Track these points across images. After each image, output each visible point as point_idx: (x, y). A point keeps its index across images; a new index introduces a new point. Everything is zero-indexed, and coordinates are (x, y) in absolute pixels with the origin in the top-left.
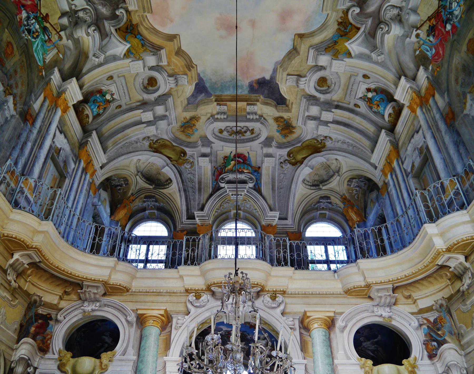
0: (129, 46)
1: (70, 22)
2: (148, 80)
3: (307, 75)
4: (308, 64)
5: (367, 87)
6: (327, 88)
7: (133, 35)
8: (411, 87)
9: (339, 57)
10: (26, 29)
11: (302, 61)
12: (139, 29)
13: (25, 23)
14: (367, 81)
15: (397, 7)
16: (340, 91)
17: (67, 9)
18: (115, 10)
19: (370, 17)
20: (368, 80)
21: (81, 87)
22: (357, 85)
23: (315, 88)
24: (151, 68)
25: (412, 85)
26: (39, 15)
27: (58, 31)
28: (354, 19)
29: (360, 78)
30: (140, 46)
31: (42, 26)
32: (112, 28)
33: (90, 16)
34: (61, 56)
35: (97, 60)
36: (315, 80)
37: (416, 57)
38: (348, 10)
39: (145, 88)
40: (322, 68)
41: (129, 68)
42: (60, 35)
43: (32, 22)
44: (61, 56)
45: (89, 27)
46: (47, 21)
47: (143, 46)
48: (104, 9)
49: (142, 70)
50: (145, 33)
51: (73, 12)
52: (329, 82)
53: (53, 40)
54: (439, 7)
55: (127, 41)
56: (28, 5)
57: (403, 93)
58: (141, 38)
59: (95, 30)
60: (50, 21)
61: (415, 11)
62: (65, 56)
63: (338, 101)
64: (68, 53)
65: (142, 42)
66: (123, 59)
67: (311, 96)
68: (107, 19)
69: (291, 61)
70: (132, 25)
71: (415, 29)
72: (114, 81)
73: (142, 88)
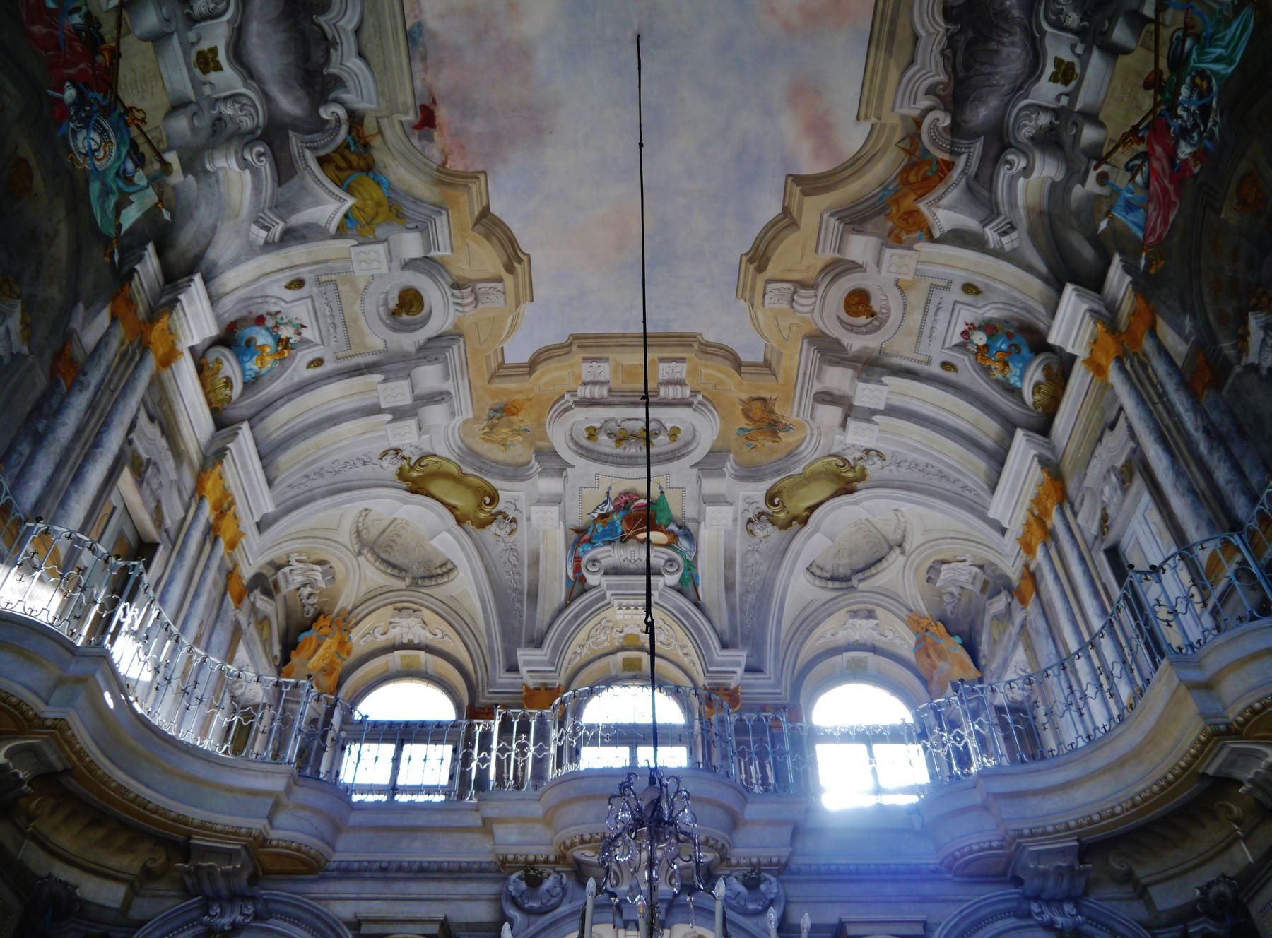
13: (1195, 135)
26: (1163, 107)
27: (1152, 27)
31: (1175, 78)
42: (1157, 11)
43: (1185, 114)
46: (1157, 71)
54: (118, 98)
60: (1152, 68)
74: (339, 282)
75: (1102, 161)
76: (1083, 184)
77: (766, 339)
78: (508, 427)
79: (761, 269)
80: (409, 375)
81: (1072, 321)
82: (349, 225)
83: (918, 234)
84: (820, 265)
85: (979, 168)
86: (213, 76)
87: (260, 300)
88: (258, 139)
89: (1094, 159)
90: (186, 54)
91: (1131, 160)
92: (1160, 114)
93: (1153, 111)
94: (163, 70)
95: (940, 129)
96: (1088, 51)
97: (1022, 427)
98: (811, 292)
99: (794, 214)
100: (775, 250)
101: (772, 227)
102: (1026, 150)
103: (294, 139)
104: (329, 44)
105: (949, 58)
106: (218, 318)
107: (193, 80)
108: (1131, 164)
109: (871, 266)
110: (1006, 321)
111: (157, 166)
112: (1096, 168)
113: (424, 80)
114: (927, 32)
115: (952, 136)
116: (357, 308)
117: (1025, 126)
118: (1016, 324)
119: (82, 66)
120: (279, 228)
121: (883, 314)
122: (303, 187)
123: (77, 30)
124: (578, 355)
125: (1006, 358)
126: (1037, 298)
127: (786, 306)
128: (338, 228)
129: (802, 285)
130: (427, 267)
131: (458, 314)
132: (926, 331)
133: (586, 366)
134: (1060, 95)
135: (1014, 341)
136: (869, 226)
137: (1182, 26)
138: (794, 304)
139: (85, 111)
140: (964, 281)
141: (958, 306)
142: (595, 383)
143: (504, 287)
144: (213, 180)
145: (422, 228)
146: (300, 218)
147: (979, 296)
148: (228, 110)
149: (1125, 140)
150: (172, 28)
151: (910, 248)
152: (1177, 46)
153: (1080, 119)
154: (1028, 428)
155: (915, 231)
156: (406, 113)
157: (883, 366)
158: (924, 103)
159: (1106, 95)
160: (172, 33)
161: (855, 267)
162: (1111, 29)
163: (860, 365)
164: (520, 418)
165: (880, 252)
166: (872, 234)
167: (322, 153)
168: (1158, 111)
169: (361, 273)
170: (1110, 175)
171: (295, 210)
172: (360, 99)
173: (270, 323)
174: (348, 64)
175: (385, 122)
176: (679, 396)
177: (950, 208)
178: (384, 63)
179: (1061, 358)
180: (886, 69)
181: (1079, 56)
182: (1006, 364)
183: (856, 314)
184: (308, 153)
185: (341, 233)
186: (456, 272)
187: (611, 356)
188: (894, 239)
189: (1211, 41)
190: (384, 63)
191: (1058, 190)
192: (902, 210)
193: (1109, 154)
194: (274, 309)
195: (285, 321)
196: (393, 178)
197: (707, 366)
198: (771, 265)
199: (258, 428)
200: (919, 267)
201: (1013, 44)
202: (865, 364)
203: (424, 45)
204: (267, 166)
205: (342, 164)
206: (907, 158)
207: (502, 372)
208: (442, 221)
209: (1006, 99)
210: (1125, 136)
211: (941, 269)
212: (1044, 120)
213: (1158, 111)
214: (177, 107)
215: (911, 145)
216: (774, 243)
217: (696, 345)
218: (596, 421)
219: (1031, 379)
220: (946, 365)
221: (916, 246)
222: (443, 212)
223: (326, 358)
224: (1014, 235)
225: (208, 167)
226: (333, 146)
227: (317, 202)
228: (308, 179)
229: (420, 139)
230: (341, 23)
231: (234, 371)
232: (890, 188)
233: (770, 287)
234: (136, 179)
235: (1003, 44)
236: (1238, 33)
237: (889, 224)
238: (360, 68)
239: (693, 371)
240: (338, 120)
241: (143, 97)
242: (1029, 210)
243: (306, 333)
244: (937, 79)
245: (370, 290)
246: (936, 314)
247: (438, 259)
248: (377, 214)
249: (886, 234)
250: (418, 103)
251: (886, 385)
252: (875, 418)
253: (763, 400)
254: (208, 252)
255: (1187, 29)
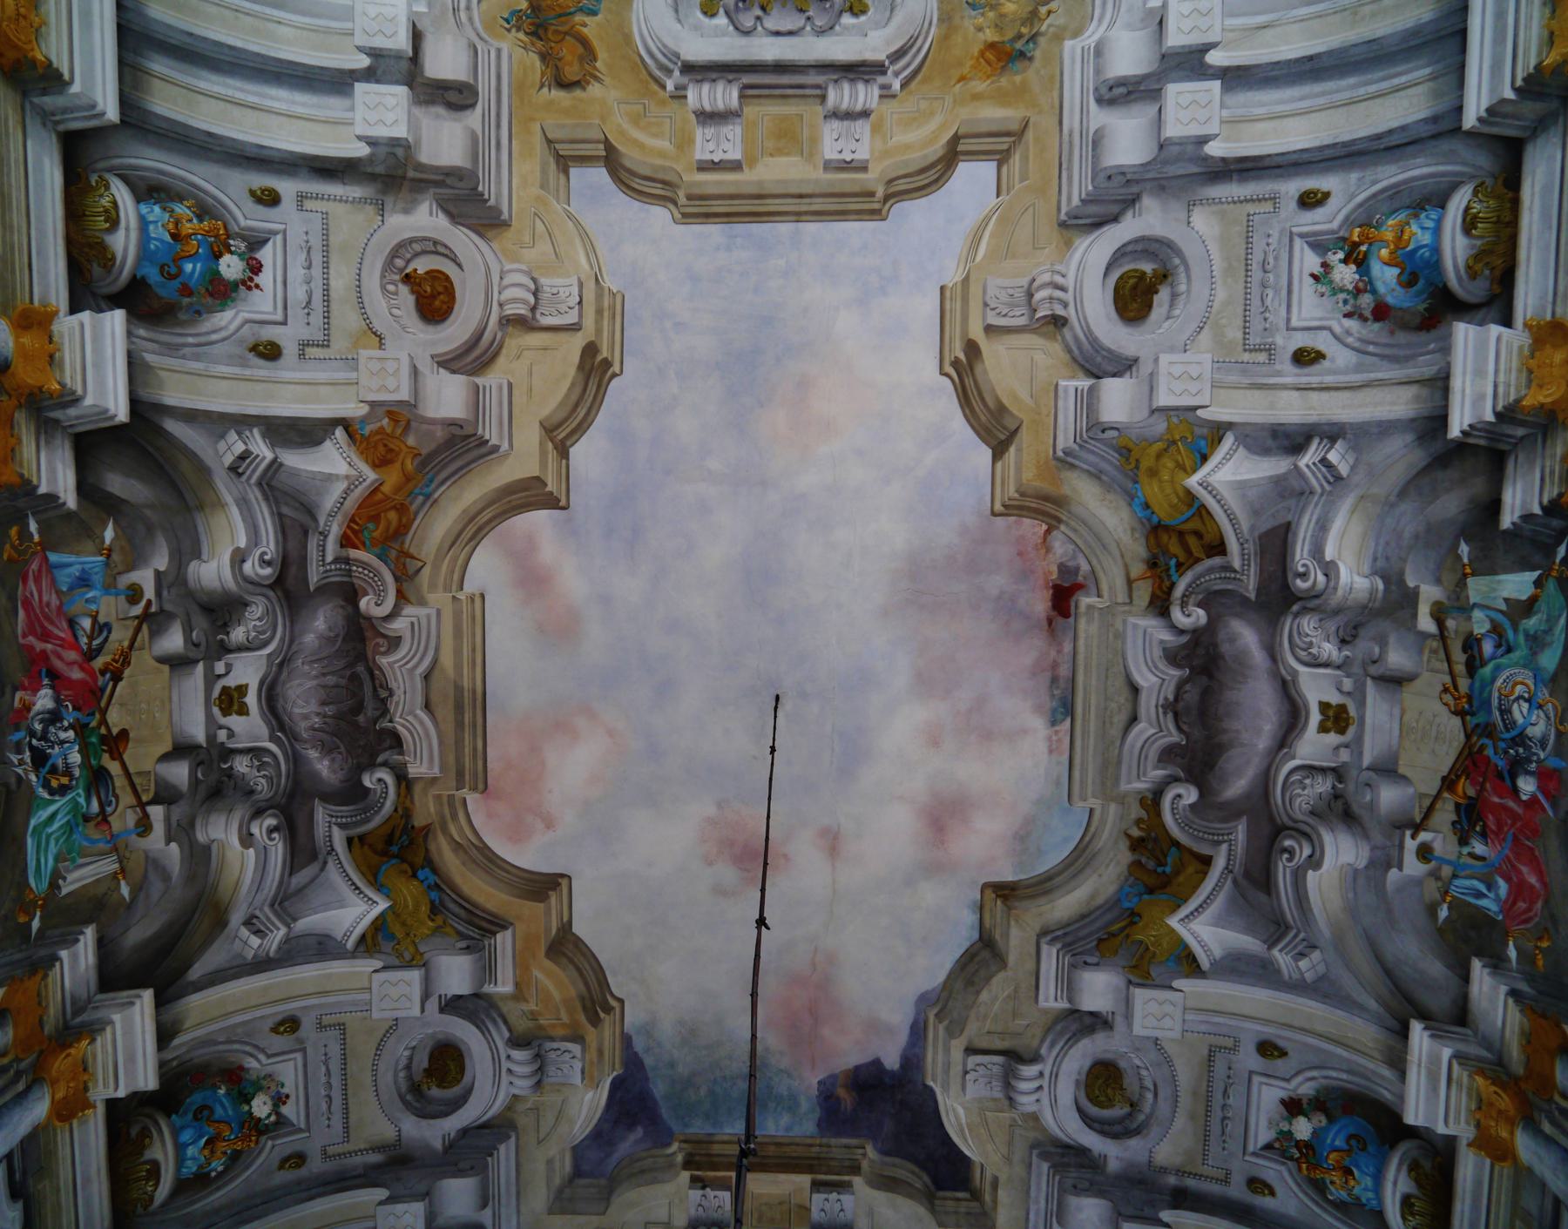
0: (383, 905)
1: (195, 782)
2: (432, 1057)
3: (1043, 1051)
4: (1042, 1003)
5: (1283, 1094)
6: (1127, 1109)
7: (405, 866)
8: (1457, 1056)
9: (1153, 974)
10: (32, 748)
11: (1016, 991)
12: (432, 847)
14: (1280, 1065)
15: (1323, 770)
16: (1180, 1122)
17: (200, 736)
18: (360, 769)
19: (1237, 815)
20: (1279, 1062)
21: (164, 1035)
22: (1244, 1089)
23: (1080, 1110)
24: (452, 1005)
25: (1462, 1047)
27: (145, 798)
28: (1184, 825)
29: (1249, 1059)
30: (425, 909)
31: (94, 762)
32: (336, 831)
33: (269, 779)
34: (125, 891)
35: (255, 941)
36: (1074, 1077)
37: (1441, 931)
38: (1158, 793)
39: (416, 1088)
40: (1097, 1022)
41: (367, 996)
44: (125, 891)
45: (258, 813)
46: (117, 755)
47: (434, 910)
48: (326, 763)
49: (416, 1012)
50: (450, 861)
51: (214, 752)
52: (1130, 1082)
53: (116, 824)
55: (379, 887)
56: (69, 680)
57: (1434, 1089)
58: (432, 879)
59: (275, 829)
60: (125, 757)
61: (1388, 770)
62: (142, 896)
63: (1180, 1172)
64: (156, 888)
65: (434, 895)
66: (353, 955)
67: (1067, 1147)
68: (327, 798)
69: (978, 993)
70: (408, 829)
71: (1408, 833)
72: (301, 1041)
73: (404, 1087)
74: (1240, 348)
75: (145, 617)
76: (158, 574)
77: (570, 216)
78: (1002, 16)
79: (590, 350)
80: (1161, 147)
81: (99, 366)
82: (1203, 443)
83: (367, 431)
84: (501, 360)
85: (305, 547)
86: (1334, 699)
87: (1371, 348)
88: (1300, 599)
89: (154, 614)
90: (1359, 739)
91: (106, 640)
92: (93, 714)
93: (104, 712)
94: (1396, 732)
95: (370, 590)
96: (211, 738)
97: (111, 128)
98: (510, 310)
99: (550, 445)
100: (573, 385)
101: (580, 425)
102: (250, 587)
103: (1251, 587)
104: (1174, 708)
105: (381, 686)
106: (1446, 350)
107: (1362, 704)
108: (105, 634)
109: (425, 366)
110: (199, 313)
111: (1451, 624)
112: (149, 602)
113: (1059, 652)
114: (416, 716)
115: (353, 585)
116: (1221, 295)
117: (260, 619)
118: (182, 316)
119: (1496, 800)
120: (1308, 459)
121: (393, 283)
122: (1256, 513)
123: (1484, 835)
124: (873, 178)
125: (179, 247)
126: (163, 374)
127: (543, 281)
128: (1220, 442)
129: (524, 324)
130: (1099, 359)
131: (1064, 271)
132: (317, 259)
133: (863, 153)
134: (227, 673)
135: (176, 284)
136: (440, 434)
137: (109, 819)
138: (533, 287)
139: (1517, 752)
140: (282, 362)
141: (279, 317)
142: (849, 116)
143: (984, 318)
144: (1380, 564)
145: (1096, 427)
146: (1272, 466)
147: (251, 341)
148: (1329, 649)
149: (125, 658)
150: (1366, 775)
151: (373, 404)
152: (107, 796)
153: (193, 654)
154: (101, 133)
155: (372, 434)
156: (1090, 607)
157: (372, 177)
158: (399, 625)
159: (170, 698)
160: (1368, 769)
161: (448, 363)
162: (193, 773)
163: (411, 174)
164: (980, 35)
165: (416, 391)
166: (433, 422)
167: (1217, 561)
168: (98, 716)
169: (1202, 359)
170: (127, 605)
171: (1278, 481)
172: (1149, 630)
173: (1366, 301)
174: (1155, 679)
175: (1122, 597)
176: (706, 87)
177: (330, 478)
178: (1107, 677)
179: (94, 295)
180: (458, 667)
181: (221, 727)
182: (176, 237)
183: (436, 276)
184: (1237, 564)
185: (1218, 431)
186: (1056, 348)
187: (820, 174)
188: (400, 415)
189: (70, 828)
190: (1107, 677)
191: (188, 549)
192: (398, 465)
193: (138, 630)
194: (1352, 324)
195: (1342, 296)
196: (1125, 513)
197: (662, 154)
198: (575, 357)
199: (1444, 105)
200: (354, 375)
201: (306, 717)
202: (404, 178)
203: (1053, 696)
204: (1298, 557)
205: (1192, 541)
206: (406, 546)
207: (1003, 143)
208: (1065, 440)
209: (294, 648)
210: (126, 662)
211: (322, 376)
212: (238, 634)
213: (98, 716)
214: (1394, 682)
215: (404, 565)
216: (574, 397)
217: (682, 200)
218: (846, 28)
219: (127, 229)
220: (270, 199)
221: (365, 409)
222: (1060, 454)
223: (1293, 205)
224: (228, 459)
225: (1381, 586)
226: (1199, 568)
227: (1241, 486)
228: (1245, 526)
229: (1077, 569)
230: (1153, 731)
231: (1453, 240)
232: (421, 498)
233: (571, 318)
234: (1487, 626)
235: (318, 714)
236: (43, 860)
237: (411, 441)
238: (1140, 672)
239: (684, 143)
240: (1184, 605)
241: (1435, 716)
242: (222, 505)
243: (1312, 262)
244: (391, 659)
245: (1194, 326)
246: (310, 294)
247: (1081, 374)
248: (1159, 456)
249: (413, 424)
250: (1071, 620)
251: (360, 138)
252: (364, 62)
253: (564, 85)
254: (1424, 463)
255: (103, 819)
